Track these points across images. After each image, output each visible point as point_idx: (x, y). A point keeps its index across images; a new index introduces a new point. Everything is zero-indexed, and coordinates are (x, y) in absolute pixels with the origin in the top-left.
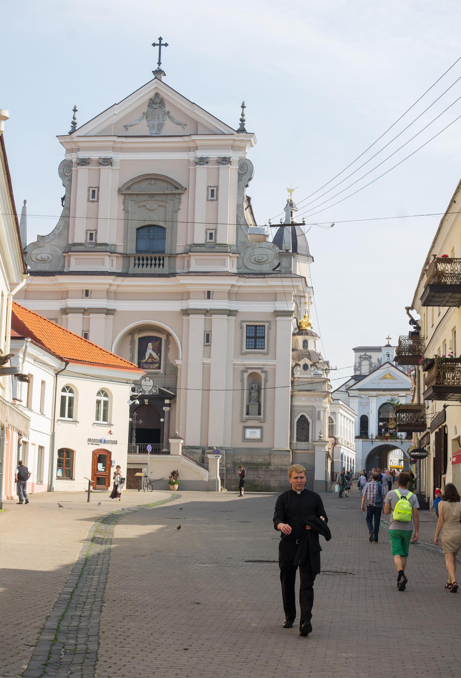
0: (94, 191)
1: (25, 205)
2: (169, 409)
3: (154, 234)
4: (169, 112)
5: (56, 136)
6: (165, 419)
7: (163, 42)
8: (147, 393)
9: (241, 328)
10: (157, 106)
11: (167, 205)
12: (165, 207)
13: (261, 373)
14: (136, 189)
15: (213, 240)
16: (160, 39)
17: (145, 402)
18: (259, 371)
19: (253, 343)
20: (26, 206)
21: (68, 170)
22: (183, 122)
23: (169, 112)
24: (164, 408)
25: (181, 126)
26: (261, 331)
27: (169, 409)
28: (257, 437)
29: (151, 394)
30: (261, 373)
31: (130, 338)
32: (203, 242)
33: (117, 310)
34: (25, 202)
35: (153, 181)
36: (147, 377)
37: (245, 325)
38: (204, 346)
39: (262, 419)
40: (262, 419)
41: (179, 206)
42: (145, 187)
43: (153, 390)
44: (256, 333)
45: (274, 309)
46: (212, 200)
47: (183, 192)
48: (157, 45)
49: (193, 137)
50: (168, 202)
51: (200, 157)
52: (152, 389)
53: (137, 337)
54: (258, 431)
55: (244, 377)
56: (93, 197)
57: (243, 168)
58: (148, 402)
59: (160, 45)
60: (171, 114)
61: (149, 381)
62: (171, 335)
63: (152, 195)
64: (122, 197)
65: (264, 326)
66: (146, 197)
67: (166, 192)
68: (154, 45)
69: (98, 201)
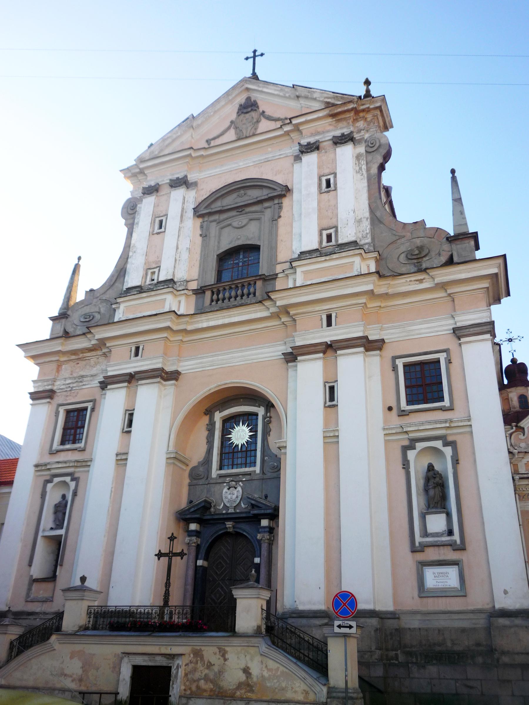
0: (161, 222)
1: (79, 262)
2: (268, 537)
3: (245, 260)
4: (263, 112)
5: (121, 171)
6: (262, 557)
7: (257, 54)
8: (231, 511)
9: (395, 368)
10: (249, 109)
11: (261, 216)
12: (258, 219)
13: (444, 446)
14: (217, 206)
15: (333, 242)
16: (255, 52)
17: (226, 528)
18: (438, 444)
20: (80, 263)
21: (133, 207)
22: (283, 117)
23: (263, 112)
24: (259, 536)
25: (281, 122)
27: (268, 537)
28: (452, 586)
29: (238, 511)
30: (444, 446)
31: (206, 420)
32: (315, 245)
33: (183, 372)
34: (79, 258)
35: (242, 192)
36: (232, 481)
37: (400, 363)
38: (325, 407)
39: (458, 542)
40: (458, 542)
41: (279, 213)
42: (229, 201)
43: (242, 504)
45: (454, 326)
46: (329, 192)
47: (283, 193)
48: (251, 58)
49: (294, 122)
50: (263, 212)
51: (306, 144)
52: (240, 502)
53: (218, 417)
54: (452, 572)
55: (409, 458)
56: (161, 227)
57: (372, 144)
58: (234, 527)
59: (254, 57)
60: (266, 113)
61: (236, 488)
62: (273, 406)
63: (240, 209)
64: (199, 221)
65: (438, 361)
66: (234, 213)
67: (259, 199)
68: (247, 59)
69: (165, 232)
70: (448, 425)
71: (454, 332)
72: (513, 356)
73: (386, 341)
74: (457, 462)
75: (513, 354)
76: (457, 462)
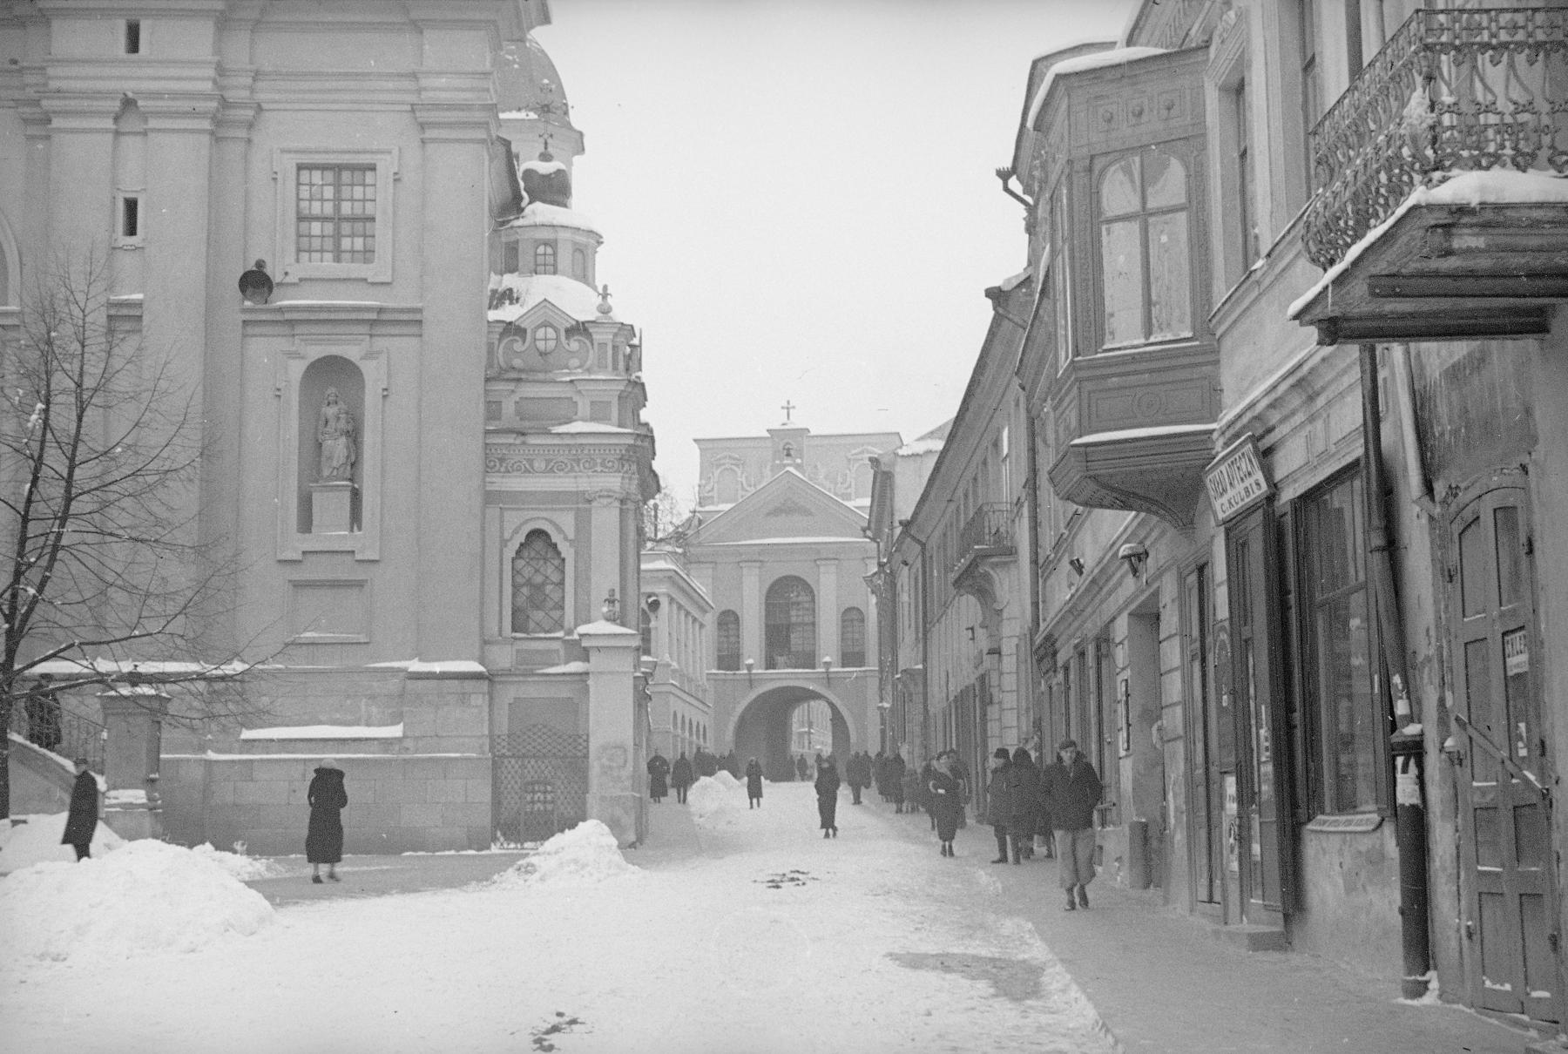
19: (329, 244)
26: (358, 192)
37: (290, 162)
44: (338, 200)
70: (373, 316)
71: (413, 111)
72: (546, 148)
73: (265, 106)
74: (385, 393)
75: (546, 143)
76: (385, 393)
